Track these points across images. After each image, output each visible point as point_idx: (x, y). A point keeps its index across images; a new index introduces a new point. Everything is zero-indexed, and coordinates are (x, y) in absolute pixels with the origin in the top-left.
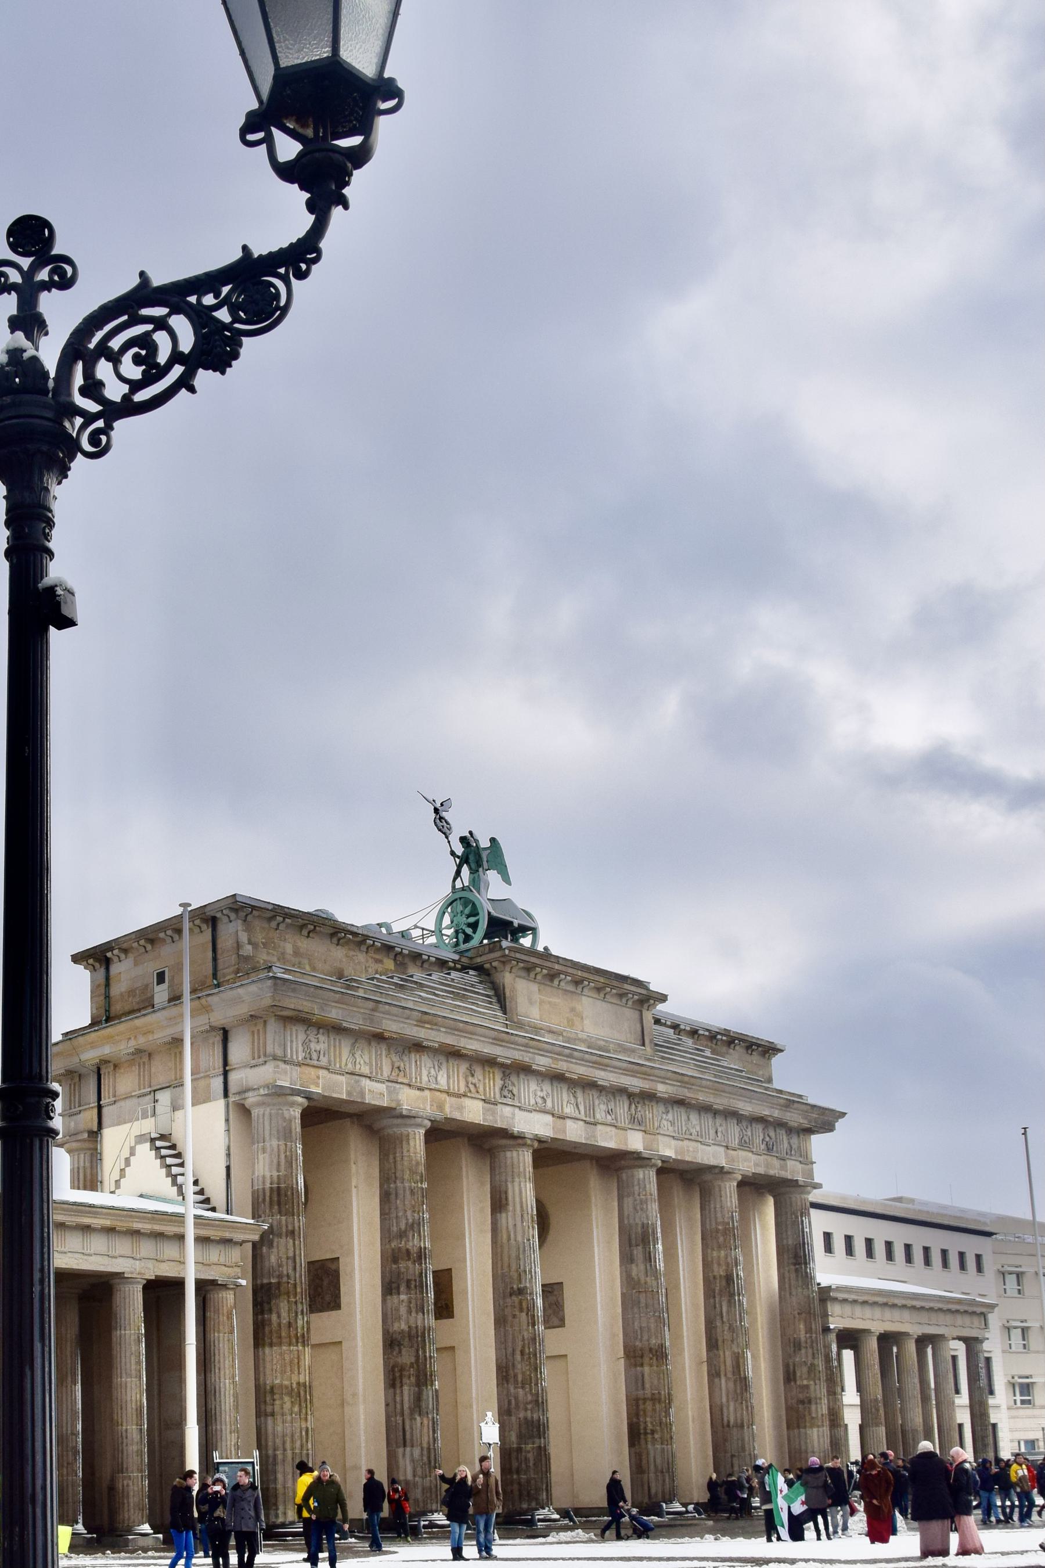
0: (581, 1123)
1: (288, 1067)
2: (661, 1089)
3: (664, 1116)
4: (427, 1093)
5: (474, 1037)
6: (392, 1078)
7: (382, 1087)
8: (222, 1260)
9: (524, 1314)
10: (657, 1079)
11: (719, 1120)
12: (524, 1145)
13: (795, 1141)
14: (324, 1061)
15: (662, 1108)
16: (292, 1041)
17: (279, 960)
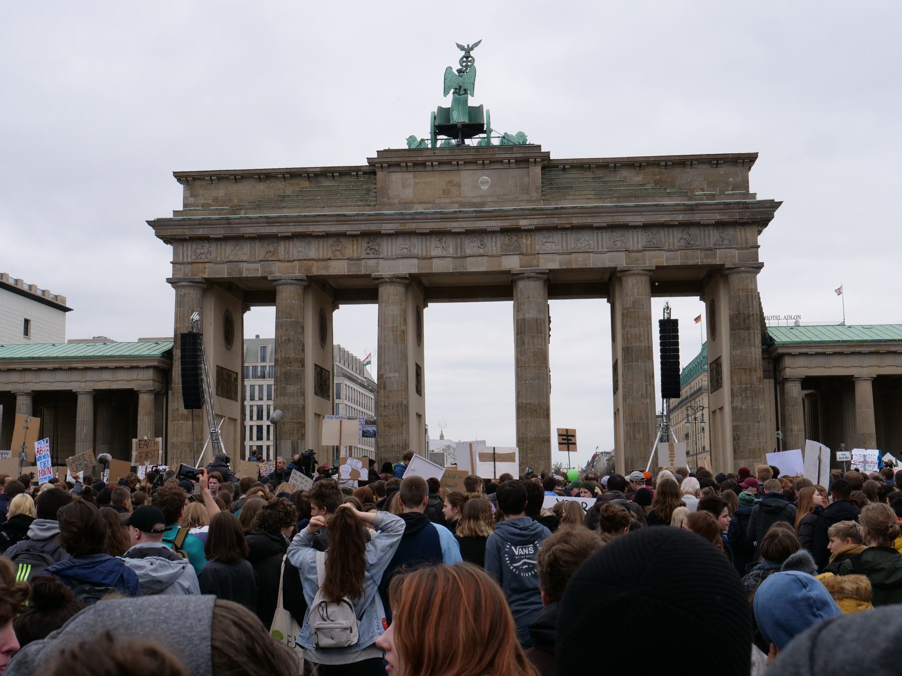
0: (450, 259)
1: (182, 266)
2: (523, 223)
3: (545, 240)
4: (295, 262)
5: (320, 223)
6: (263, 259)
7: (258, 266)
8: (140, 377)
9: (382, 391)
10: (516, 217)
11: (617, 235)
12: (386, 282)
13: (730, 232)
14: (210, 258)
15: (546, 234)
16: (183, 251)
17: (213, 201)
